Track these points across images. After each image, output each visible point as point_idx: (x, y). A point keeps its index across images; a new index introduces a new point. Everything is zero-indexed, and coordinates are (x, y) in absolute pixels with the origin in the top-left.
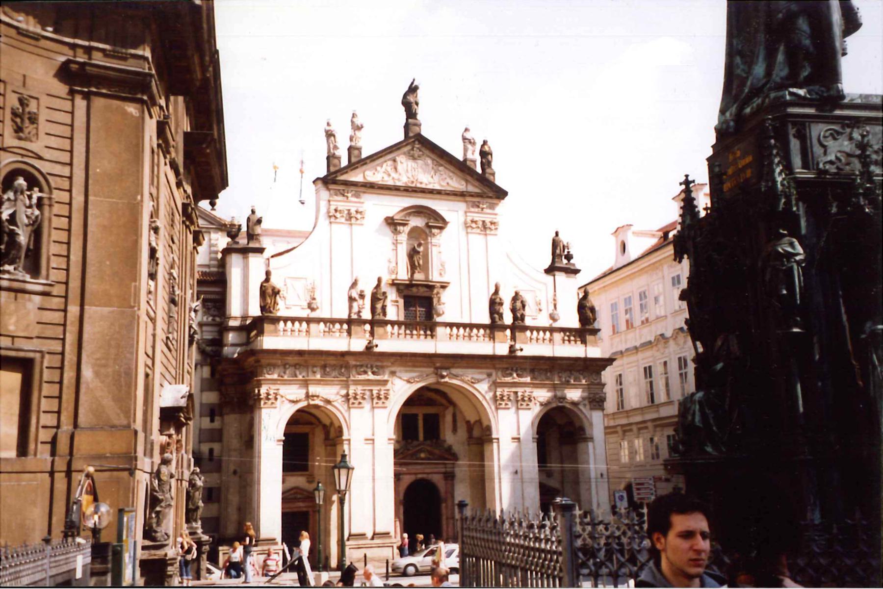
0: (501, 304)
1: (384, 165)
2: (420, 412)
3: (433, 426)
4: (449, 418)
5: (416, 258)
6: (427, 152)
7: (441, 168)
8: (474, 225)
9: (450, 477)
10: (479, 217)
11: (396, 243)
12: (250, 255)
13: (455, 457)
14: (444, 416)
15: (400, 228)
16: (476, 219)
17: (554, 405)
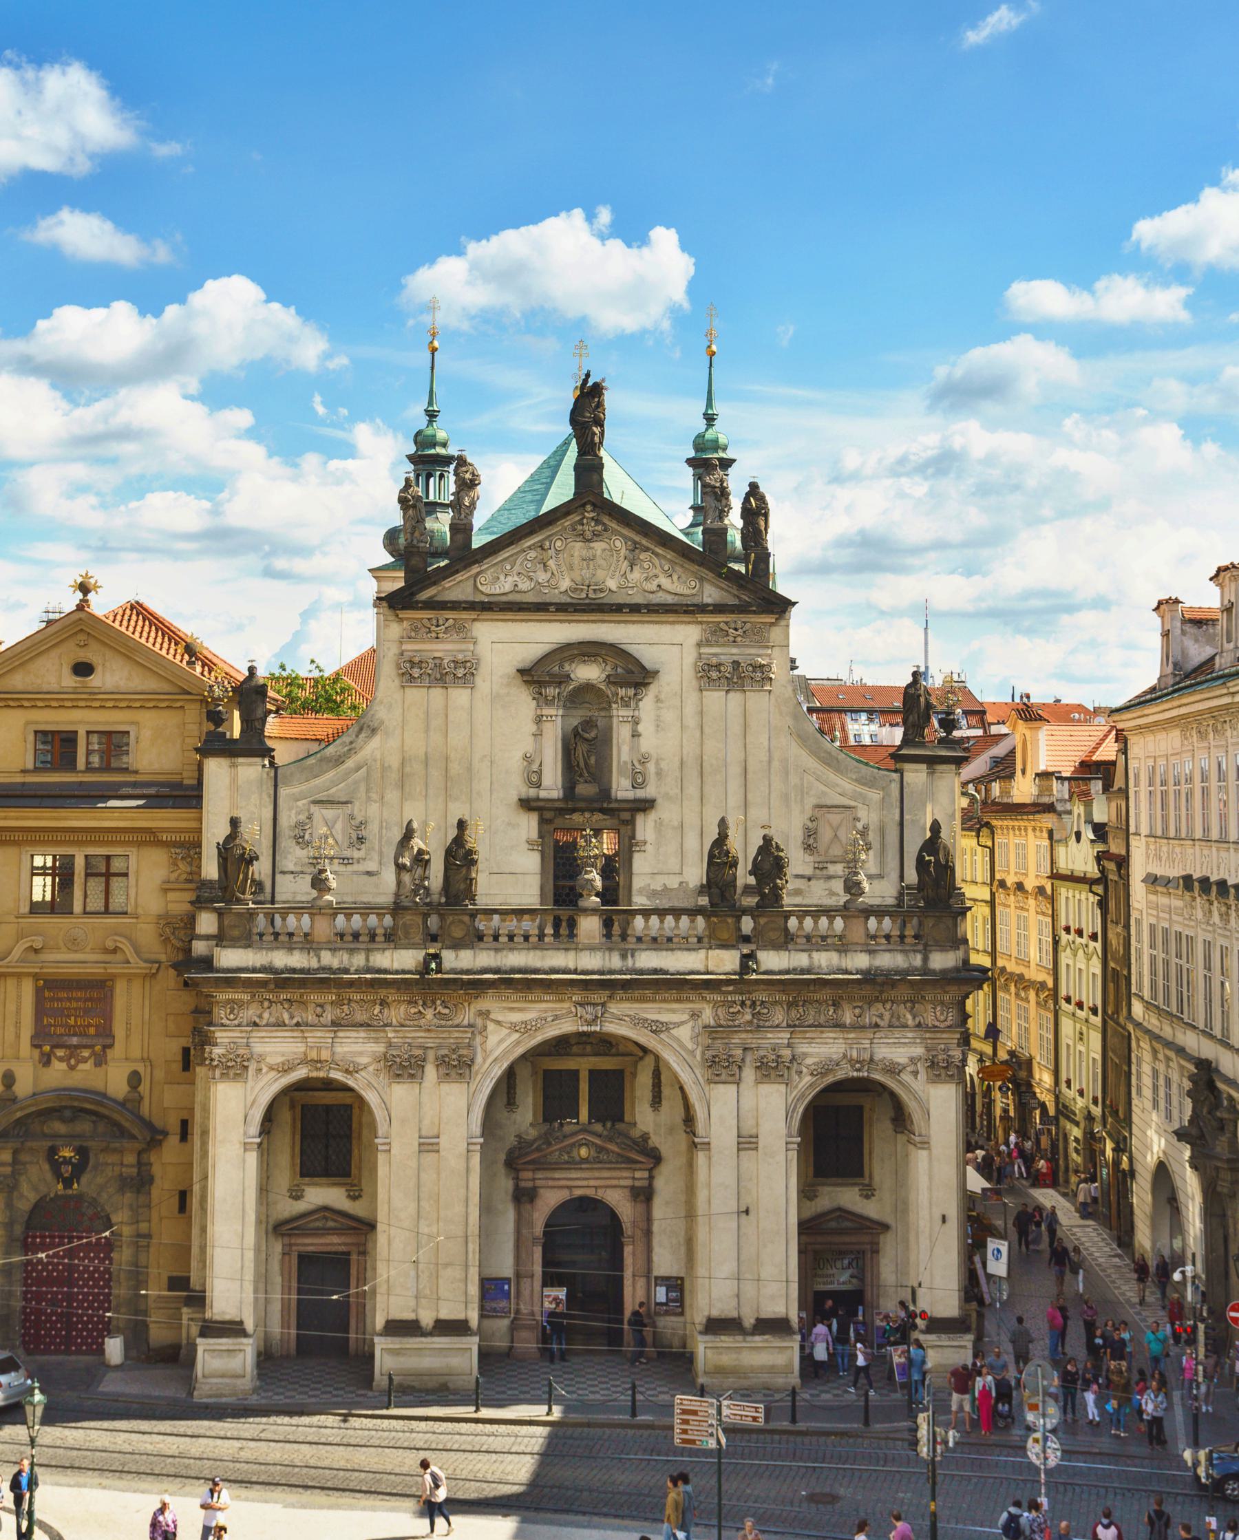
0: (734, 864)
1: (519, 562)
2: (584, 1065)
3: (610, 1096)
4: (644, 1079)
5: (585, 752)
6: (613, 525)
7: (643, 556)
8: (714, 675)
9: (644, 1195)
10: (725, 653)
11: (539, 720)
12: (241, 760)
13: (656, 1158)
14: (634, 1075)
15: (551, 691)
16: (723, 658)
17: (840, 1075)
